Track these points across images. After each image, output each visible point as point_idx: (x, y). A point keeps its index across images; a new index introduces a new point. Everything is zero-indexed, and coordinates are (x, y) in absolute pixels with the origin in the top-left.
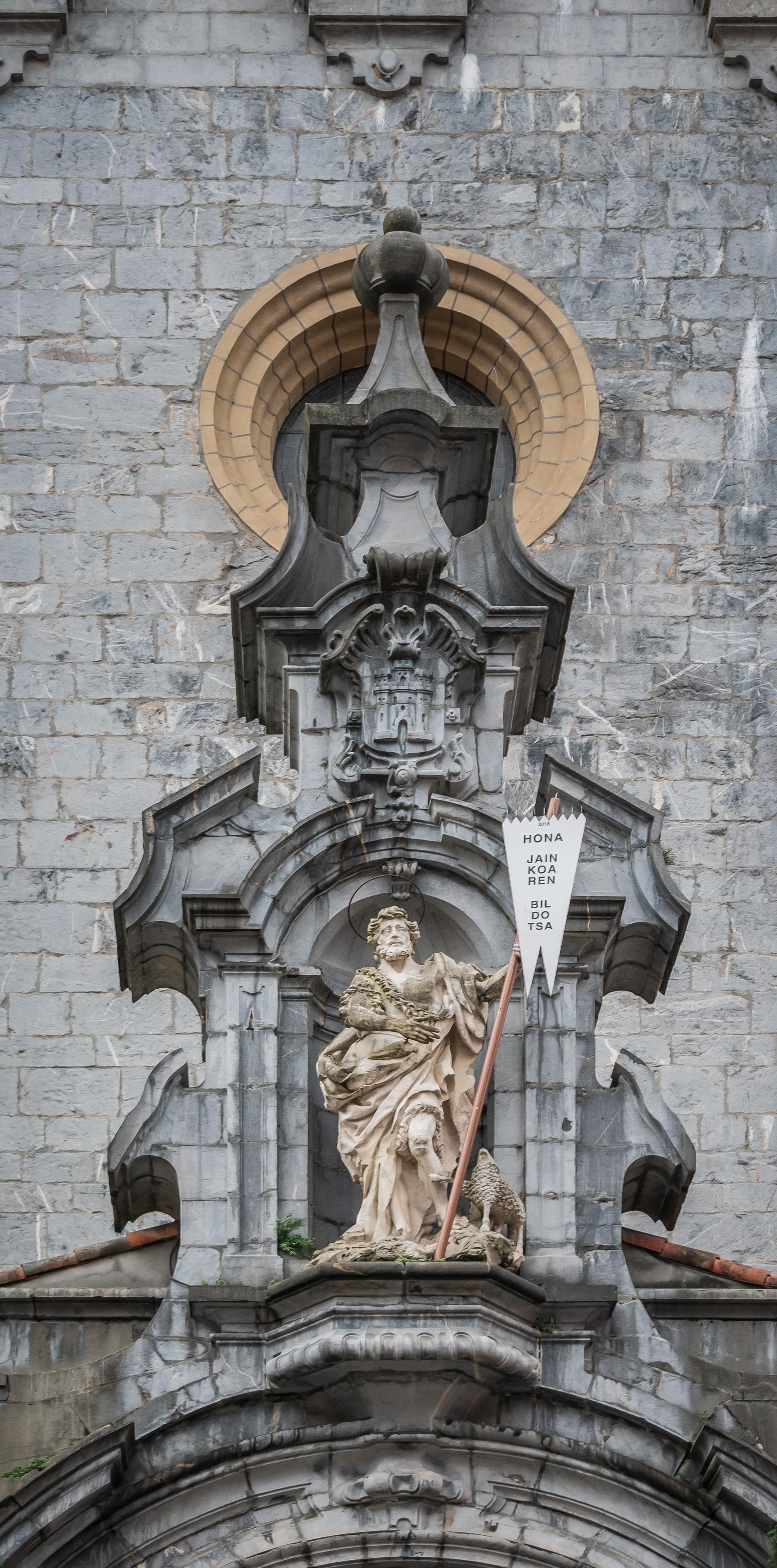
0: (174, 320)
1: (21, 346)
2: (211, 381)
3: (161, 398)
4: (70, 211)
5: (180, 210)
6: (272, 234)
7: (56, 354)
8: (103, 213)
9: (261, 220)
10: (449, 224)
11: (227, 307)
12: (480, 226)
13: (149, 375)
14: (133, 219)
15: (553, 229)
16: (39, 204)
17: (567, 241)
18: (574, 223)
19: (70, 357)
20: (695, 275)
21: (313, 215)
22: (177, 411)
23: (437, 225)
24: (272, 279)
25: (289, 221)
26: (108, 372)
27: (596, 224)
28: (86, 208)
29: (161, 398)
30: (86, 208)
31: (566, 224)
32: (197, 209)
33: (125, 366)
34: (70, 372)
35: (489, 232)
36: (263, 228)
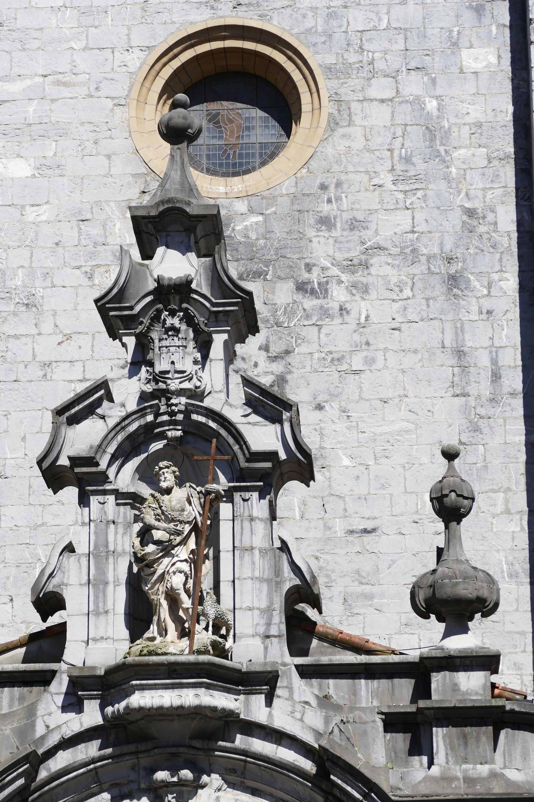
0: (117, 63)
1: (42, 79)
2: (134, 94)
3: (110, 103)
4: (67, 10)
5: (120, 7)
6: (165, 17)
7: (59, 83)
8: (83, 11)
9: (160, 10)
10: (252, 8)
11: (142, 55)
12: (267, 8)
13: (103, 93)
14: (98, 12)
15: (303, 8)
16: (52, 7)
17: (310, 14)
18: (314, 5)
19: (65, 84)
20: (375, 29)
21: (185, 7)
22: (118, 110)
23: (246, 9)
24: (165, 41)
25: (174, 10)
26: (84, 91)
27: (325, 5)
28: (75, 8)
29: (110, 103)
30: (75, 8)
31: (309, 6)
32: (128, 6)
33: (92, 89)
34: (65, 92)
35: (272, 11)
36: (160, 14)
